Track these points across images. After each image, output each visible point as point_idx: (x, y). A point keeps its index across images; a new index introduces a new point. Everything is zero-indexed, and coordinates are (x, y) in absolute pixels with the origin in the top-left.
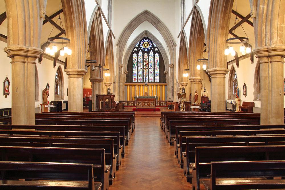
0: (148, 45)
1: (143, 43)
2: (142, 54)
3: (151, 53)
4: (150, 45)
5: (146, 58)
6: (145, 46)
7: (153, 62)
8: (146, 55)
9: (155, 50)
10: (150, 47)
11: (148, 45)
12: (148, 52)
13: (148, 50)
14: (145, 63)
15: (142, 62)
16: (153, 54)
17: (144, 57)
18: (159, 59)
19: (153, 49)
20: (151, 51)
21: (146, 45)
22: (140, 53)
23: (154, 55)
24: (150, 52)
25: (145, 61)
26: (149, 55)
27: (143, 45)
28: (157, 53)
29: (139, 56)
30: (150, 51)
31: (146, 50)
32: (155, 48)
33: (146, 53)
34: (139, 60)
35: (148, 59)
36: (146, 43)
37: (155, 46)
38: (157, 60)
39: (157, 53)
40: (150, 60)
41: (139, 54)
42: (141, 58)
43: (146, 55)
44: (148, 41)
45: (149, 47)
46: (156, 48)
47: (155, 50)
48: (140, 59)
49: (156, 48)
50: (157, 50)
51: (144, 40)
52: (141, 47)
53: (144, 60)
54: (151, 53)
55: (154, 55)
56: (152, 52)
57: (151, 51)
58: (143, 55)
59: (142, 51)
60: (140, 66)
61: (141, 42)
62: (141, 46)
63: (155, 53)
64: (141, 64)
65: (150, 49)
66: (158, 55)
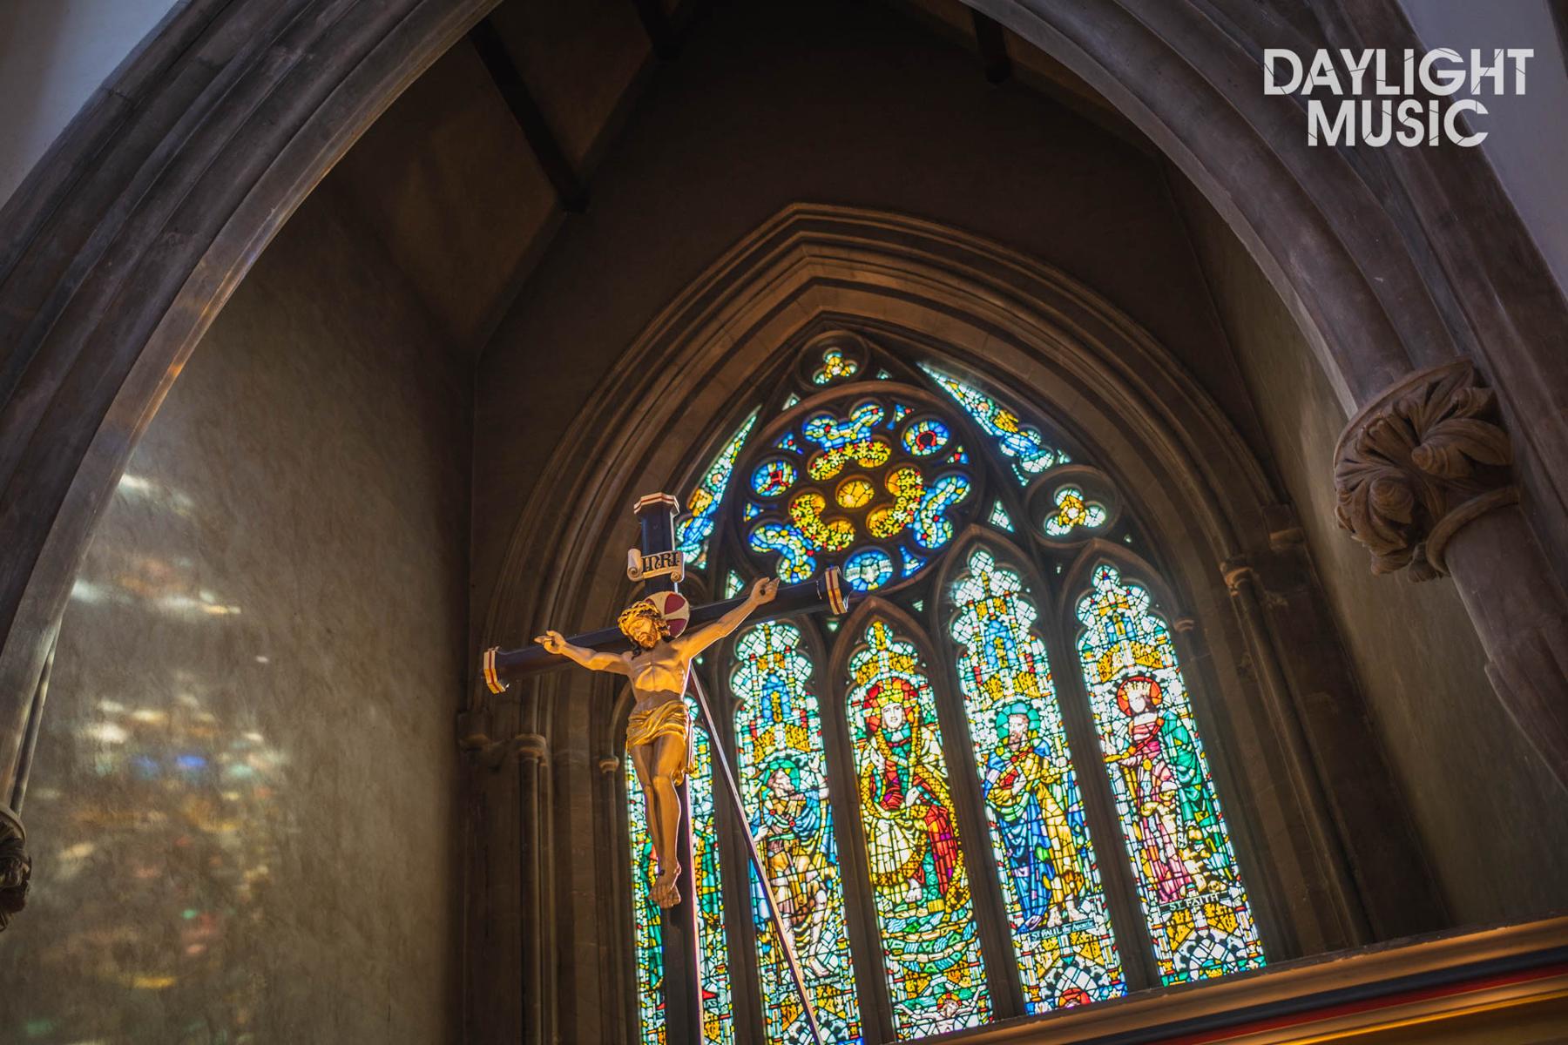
0: (903, 483)
1: (804, 484)
2: (801, 668)
3: (987, 593)
4: (932, 471)
5: (893, 717)
6: (832, 513)
7: (1061, 763)
8: (884, 656)
9: (1054, 528)
10: (952, 513)
11: (903, 483)
12: (920, 609)
13: (911, 566)
14: (891, 843)
15: (820, 818)
16: (1025, 614)
17: (857, 718)
18: (1176, 689)
19: (1000, 519)
20: (981, 562)
21: (855, 495)
22: (771, 659)
23: (1059, 631)
24: (964, 592)
25: (895, 789)
26: (939, 661)
27: (807, 509)
28: (1106, 583)
29: (742, 720)
30: (947, 565)
31: (870, 573)
32: (1034, 503)
33: (878, 632)
34: (749, 790)
35: (932, 742)
36: (851, 470)
37: (1039, 464)
38: (1136, 695)
39: (1106, 583)
40: (983, 734)
41: (744, 684)
42: (782, 752)
43: (884, 656)
44: (877, 432)
45: (925, 510)
46: (1067, 499)
47: (1054, 528)
48: (765, 775)
49: (1067, 499)
50: (1096, 518)
51: (815, 430)
52: (776, 555)
53: (869, 760)
54: (987, 593)
55: (1059, 631)
56: (1005, 582)
57: (981, 562)
58: (831, 686)
59: (800, 605)
60: (801, 912)
61: (761, 484)
62: (765, 539)
63: (1055, 579)
64: (815, 867)
65: (937, 535)
66: (1140, 598)
